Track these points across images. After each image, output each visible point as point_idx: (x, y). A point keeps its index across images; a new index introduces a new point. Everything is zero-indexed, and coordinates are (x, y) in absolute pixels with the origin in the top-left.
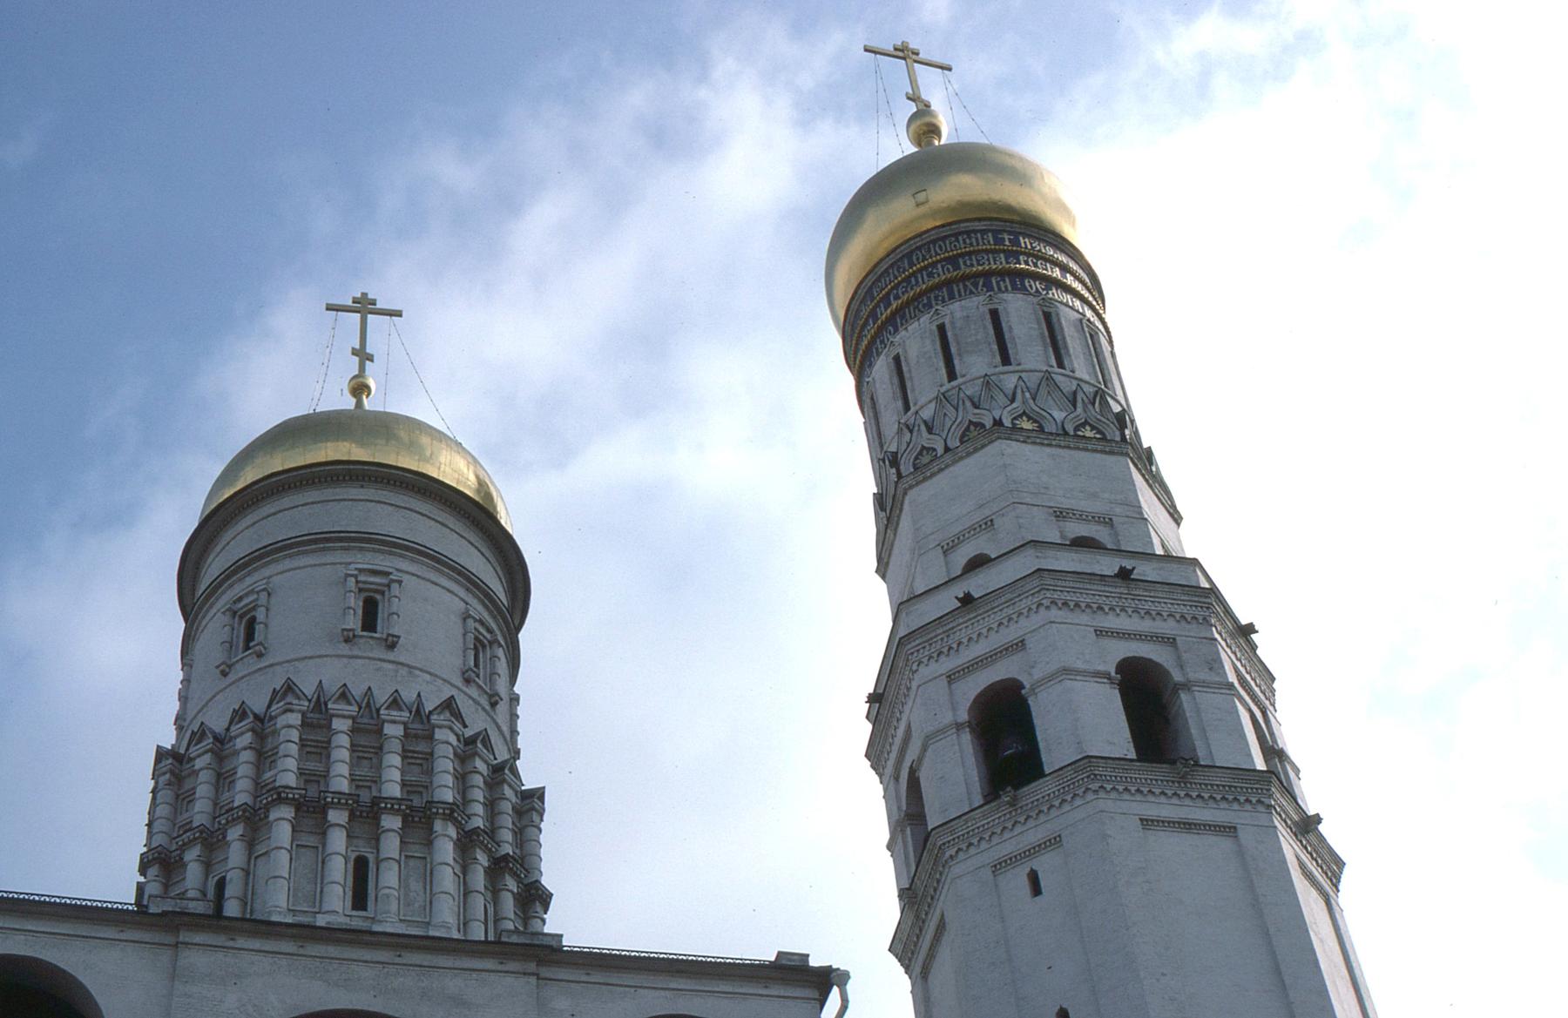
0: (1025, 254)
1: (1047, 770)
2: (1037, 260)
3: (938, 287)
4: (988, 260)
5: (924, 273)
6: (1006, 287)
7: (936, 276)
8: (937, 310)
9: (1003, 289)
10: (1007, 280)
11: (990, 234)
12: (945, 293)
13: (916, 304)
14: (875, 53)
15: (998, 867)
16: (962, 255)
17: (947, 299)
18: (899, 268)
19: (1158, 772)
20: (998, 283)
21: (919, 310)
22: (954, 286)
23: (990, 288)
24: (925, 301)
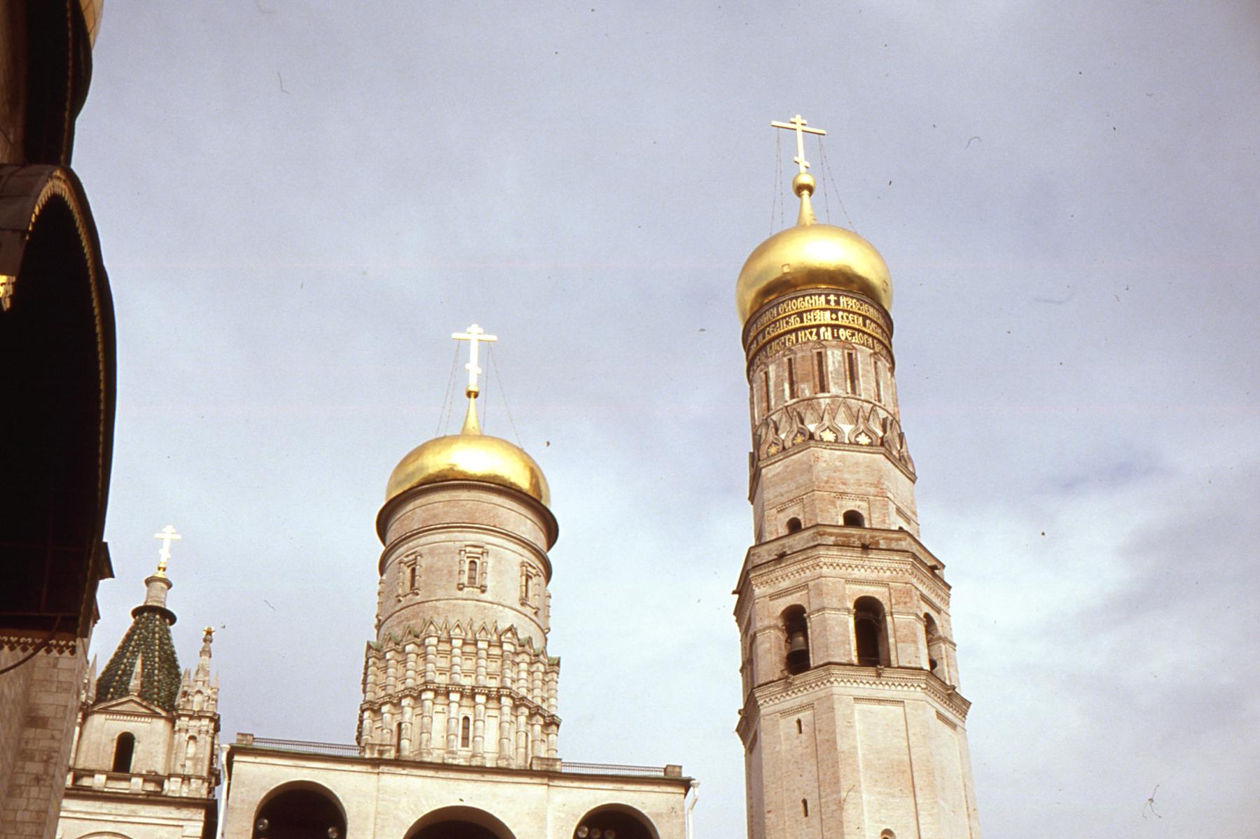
0: (844, 311)
1: (812, 665)
3: (790, 332)
15: (785, 713)
18: (771, 313)
19: (869, 672)
24: (783, 341)
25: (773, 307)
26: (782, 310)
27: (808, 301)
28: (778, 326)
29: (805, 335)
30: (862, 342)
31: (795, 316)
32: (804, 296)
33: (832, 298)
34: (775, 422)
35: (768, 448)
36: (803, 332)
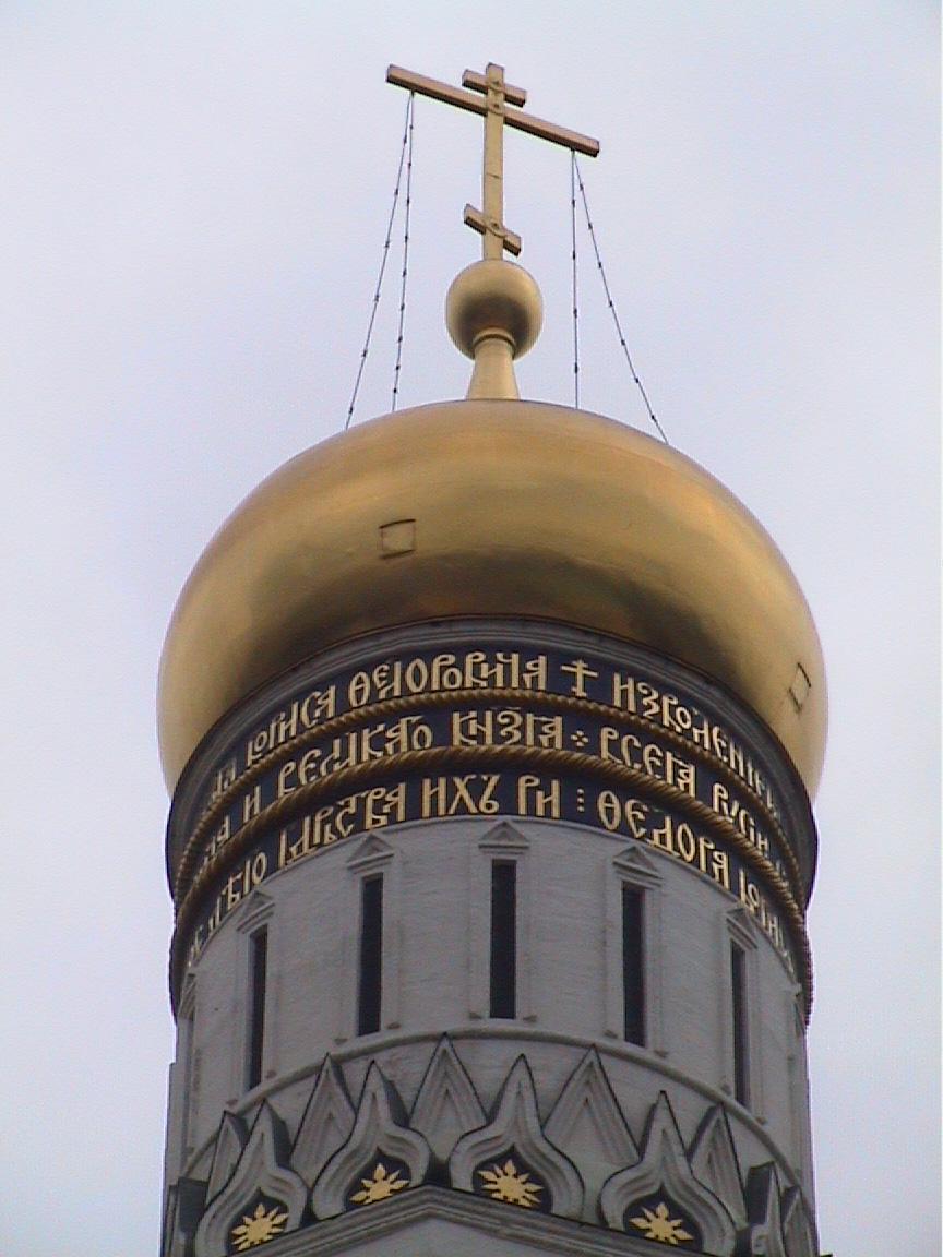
0: (625, 727)
2: (644, 744)
3: (384, 776)
4: (522, 728)
5: (366, 734)
6: (548, 806)
7: (390, 747)
8: (372, 838)
9: (540, 811)
10: (555, 785)
11: (542, 660)
12: (401, 799)
13: (331, 810)
14: (415, 88)
16: (464, 705)
17: (401, 816)
18: (313, 706)
20: (531, 792)
21: (334, 830)
22: (427, 783)
23: (509, 807)
24: (352, 810)
25: (322, 686)
26: (359, 693)
27: (477, 667)
28: (336, 754)
29: (452, 790)
30: (689, 857)
31: (414, 719)
32: (461, 651)
33: (580, 669)
34: (280, 1126)
35: (239, 1222)
36: (442, 782)
